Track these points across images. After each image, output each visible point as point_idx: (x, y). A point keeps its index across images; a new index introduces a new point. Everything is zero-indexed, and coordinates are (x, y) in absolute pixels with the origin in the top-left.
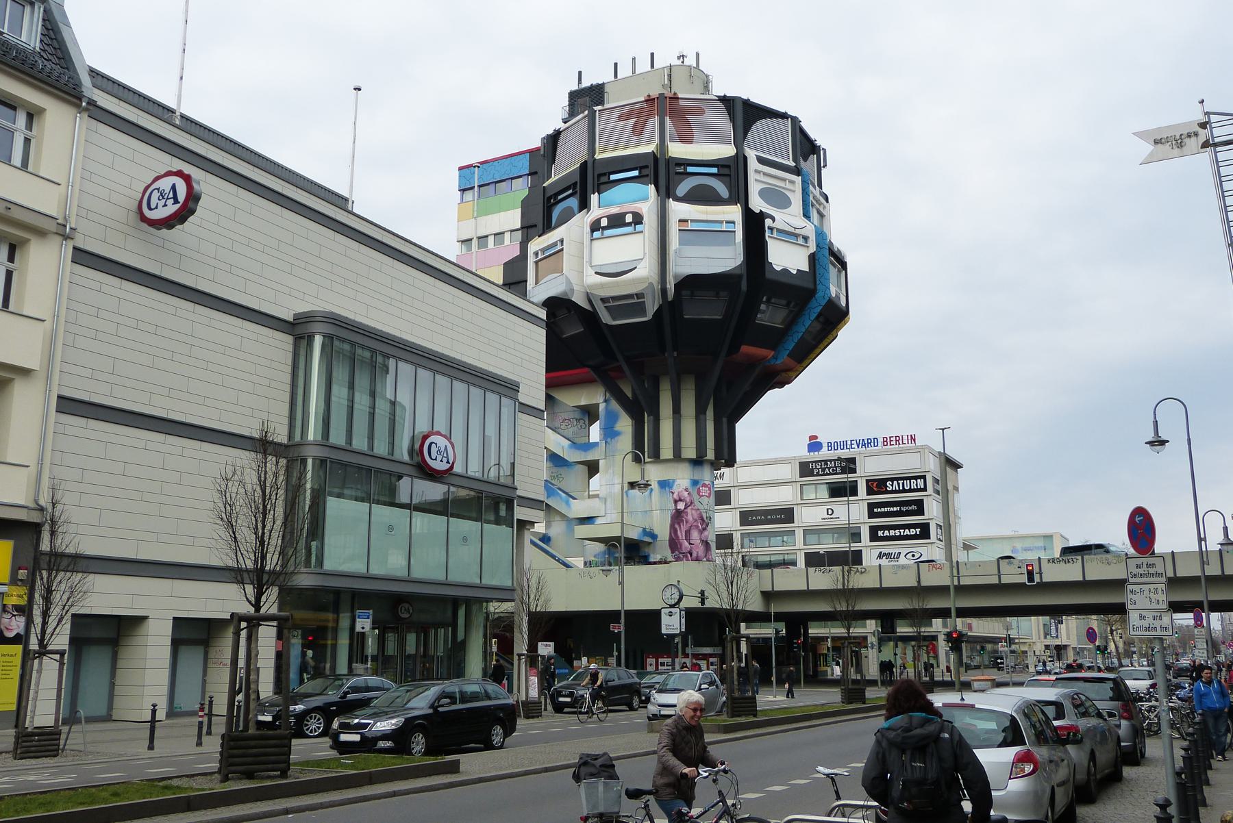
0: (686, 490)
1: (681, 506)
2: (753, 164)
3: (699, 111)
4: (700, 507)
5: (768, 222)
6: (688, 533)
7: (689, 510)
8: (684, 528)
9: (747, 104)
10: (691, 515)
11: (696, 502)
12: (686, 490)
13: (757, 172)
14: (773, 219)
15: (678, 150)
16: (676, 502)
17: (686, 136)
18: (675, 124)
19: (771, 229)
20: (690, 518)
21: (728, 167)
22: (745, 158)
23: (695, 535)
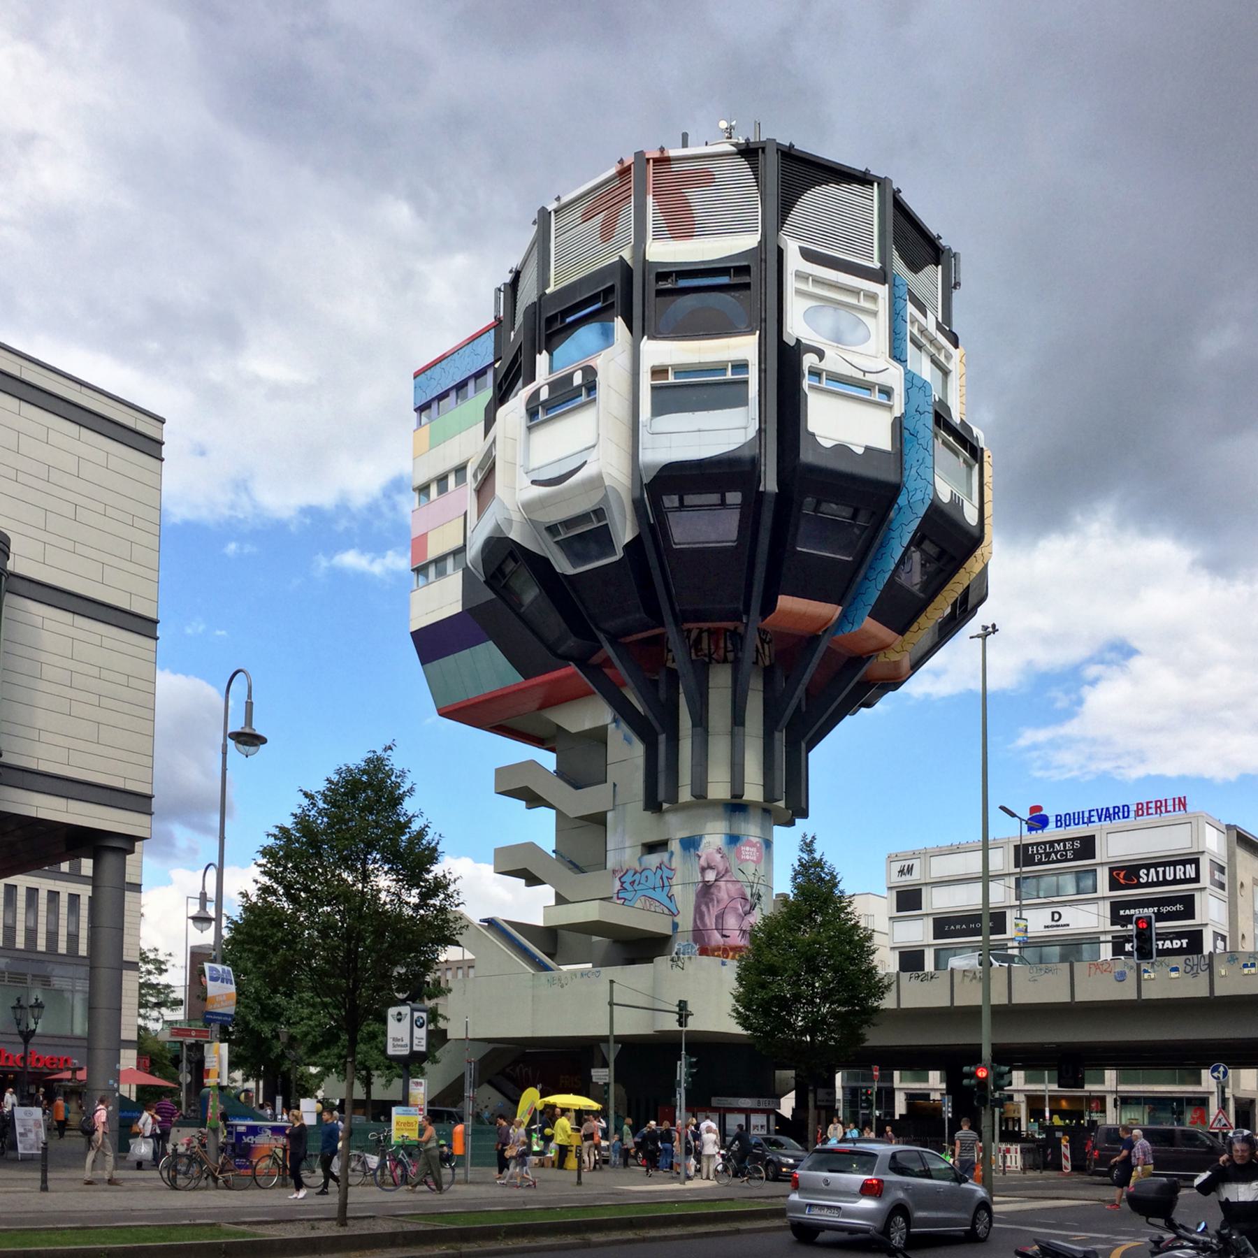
0: (719, 850)
1: (711, 876)
2: (794, 262)
3: (706, 179)
4: (741, 877)
5: (809, 360)
6: (720, 917)
7: (722, 884)
8: (715, 911)
9: (789, 156)
10: (724, 891)
11: (734, 870)
12: (719, 850)
13: (800, 276)
14: (821, 354)
15: (662, 251)
16: (703, 870)
17: (681, 224)
18: (662, 208)
19: (816, 373)
20: (723, 895)
21: (745, 270)
22: (780, 252)
23: (731, 922)
